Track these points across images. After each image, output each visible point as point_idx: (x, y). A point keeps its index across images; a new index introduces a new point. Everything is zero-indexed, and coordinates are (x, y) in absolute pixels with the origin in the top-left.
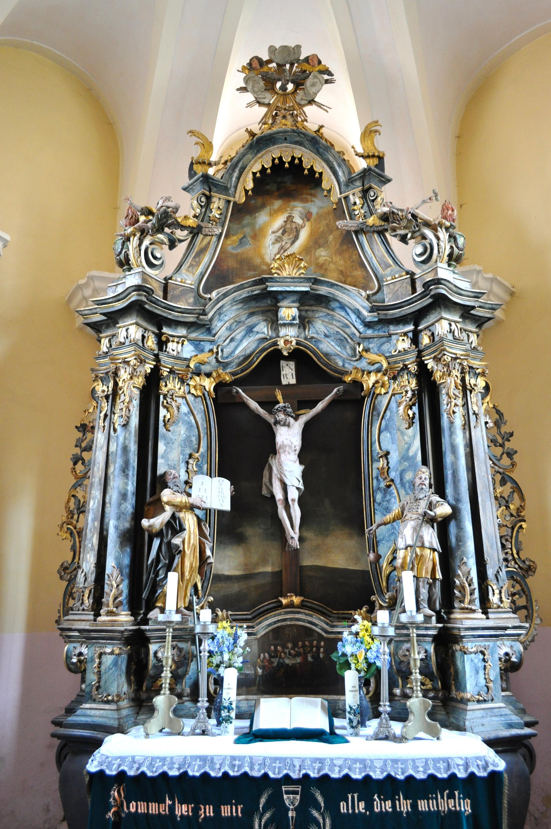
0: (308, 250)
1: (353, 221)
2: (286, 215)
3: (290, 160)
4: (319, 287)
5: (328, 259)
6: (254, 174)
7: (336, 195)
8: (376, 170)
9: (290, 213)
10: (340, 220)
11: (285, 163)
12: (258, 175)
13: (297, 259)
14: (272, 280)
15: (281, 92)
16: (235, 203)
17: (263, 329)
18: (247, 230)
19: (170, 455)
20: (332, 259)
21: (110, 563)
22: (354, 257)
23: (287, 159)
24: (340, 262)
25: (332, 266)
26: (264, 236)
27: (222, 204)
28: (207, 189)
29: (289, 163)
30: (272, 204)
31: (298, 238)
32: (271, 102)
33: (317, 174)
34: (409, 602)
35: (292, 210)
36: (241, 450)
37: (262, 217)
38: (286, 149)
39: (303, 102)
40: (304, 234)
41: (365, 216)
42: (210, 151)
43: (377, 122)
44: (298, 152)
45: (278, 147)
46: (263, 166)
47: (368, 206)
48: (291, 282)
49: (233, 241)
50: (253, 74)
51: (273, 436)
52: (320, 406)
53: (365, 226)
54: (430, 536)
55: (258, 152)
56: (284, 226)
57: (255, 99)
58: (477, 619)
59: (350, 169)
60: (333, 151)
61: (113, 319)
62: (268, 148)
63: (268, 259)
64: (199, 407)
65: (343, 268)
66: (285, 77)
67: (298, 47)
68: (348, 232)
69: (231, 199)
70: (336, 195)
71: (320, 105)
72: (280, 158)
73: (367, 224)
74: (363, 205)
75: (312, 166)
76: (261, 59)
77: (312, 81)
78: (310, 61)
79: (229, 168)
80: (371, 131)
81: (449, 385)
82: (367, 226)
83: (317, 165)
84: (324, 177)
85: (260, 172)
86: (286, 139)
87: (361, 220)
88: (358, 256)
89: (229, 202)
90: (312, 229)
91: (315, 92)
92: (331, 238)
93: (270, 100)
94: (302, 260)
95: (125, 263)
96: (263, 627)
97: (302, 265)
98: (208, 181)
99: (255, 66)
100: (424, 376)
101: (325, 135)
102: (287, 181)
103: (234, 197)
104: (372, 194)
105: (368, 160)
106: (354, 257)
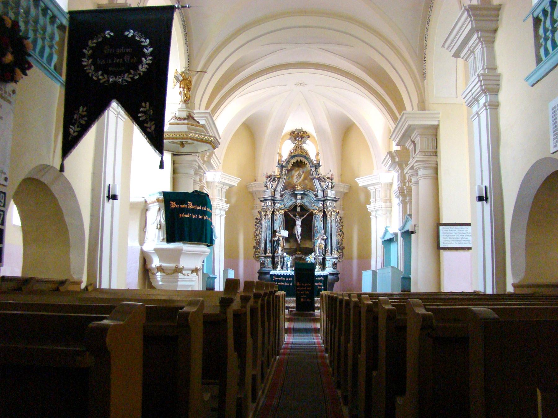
0: (303, 180)
17: (294, 200)
18: (290, 175)
19: (276, 227)
21: (268, 246)
34: (318, 252)
36: (289, 225)
37: (293, 172)
40: (302, 177)
44: (302, 158)
51: (295, 222)
52: (305, 216)
54: (323, 241)
58: (330, 255)
61: (266, 200)
63: (295, 182)
64: (281, 216)
81: (328, 214)
95: (266, 186)
96: (294, 257)
100: (324, 212)
102: (299, 165)
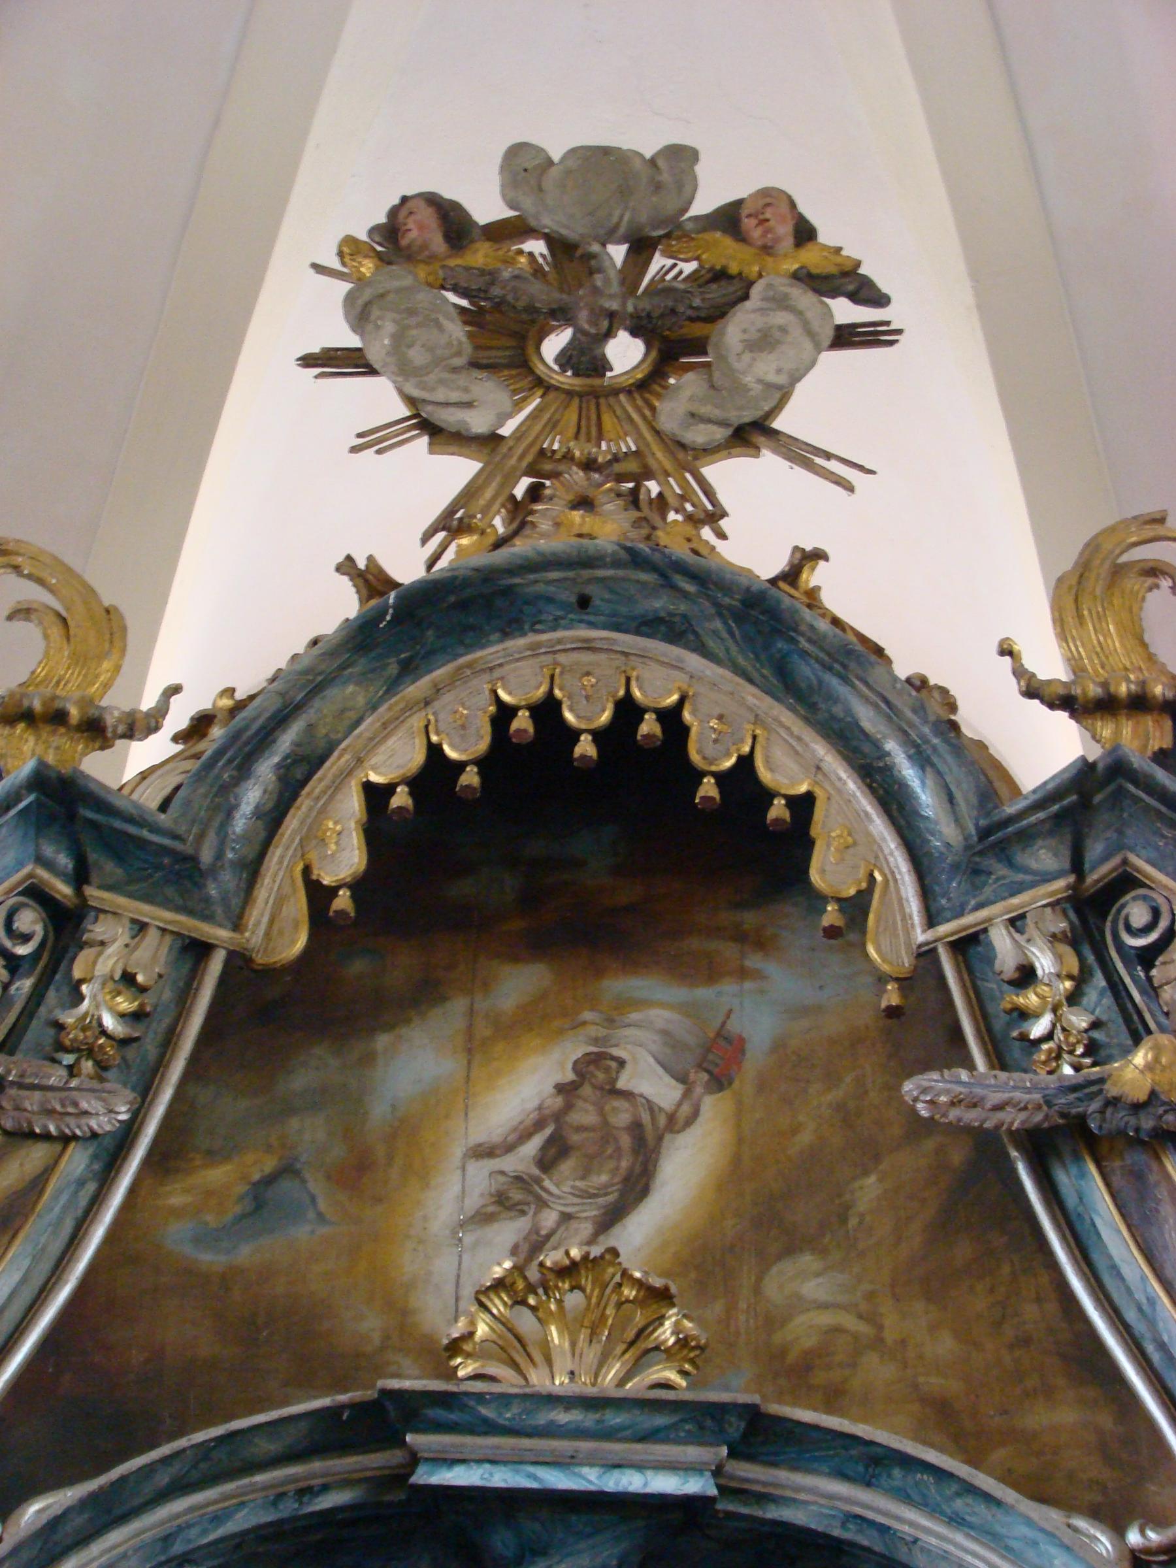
1: (1017, 1075)
2: (575, 1049)
3: (605, 717)
4: (783, 1475)
5: (850, 1322)
6: (376, 795)
7: (904, 925)
8: (1161, 775)
9: (596, 1041)
10: (925, 1066)
11: (574, 735)
12: (401, 798)
13: (629, 1292)
14: (448, 1410)
15: (567, 379)
16: (238, 961)
18: (310, 1133)
20: (881, 1328)
22: (1030, 1311)
23: (587, 714)
24: (934, 1343)
25: (877, 1371)
26: (421, 1173)
27: (151, 959)
28: (64, 861)
29: (599, 736)
30: (486, 986)
31: (645, 1192)
32: (506, 430)
33: (779, 802)
35: (610, 1022)
37: (414, 1062)
38: (586, 657)
39: (699, 435)
40: (686, 1171)
41: (1092, 1049)
42: (101, 657)
43: (1161, 520)
45: (534, 647)
46: (434, 751)
47: (1116, 987)
48: (579, 1433)
49: (209, 1193)
50: (401, 277)
53: (1095, 1106)
55: (409, 670)
56: (558, 1117)
57: (404, 411)
59: (986, 774)
60: (877, 674)
62: (470, 648)
65: (952, 1386)
66: (602, 307)
67: (681, 158)
68: (987, 1147)
69: (220, 934)
70: (904, 925)
71: (802, 454)
72: (547, 710)
73: (1112, 1090)
74: (1081, 980)
75: (746, 763)
76: (456, 207)
77: (760, 321)
78: (748, 224)
79: (219, 753)
80: (1118, 571)
82: (1113, 1102)
83: (779, 754)
84: (822, 823)
85: (416, 783)
86: (584, 602)
87: (1067, 1070)
88: (1052, 1307)
89: (196, 951)
90: (740, 1140)
91: (772, 378)
92: (868, 1190)
93: (503, 418)
94: (663, 1296)
97: (666, 1334)
98: (72, 816)
99: (416, 241)
101: (832, 601)
103: (237, 925)
104: (1138, 915)
105: (1106, 730)
106: (1030, 1311)
